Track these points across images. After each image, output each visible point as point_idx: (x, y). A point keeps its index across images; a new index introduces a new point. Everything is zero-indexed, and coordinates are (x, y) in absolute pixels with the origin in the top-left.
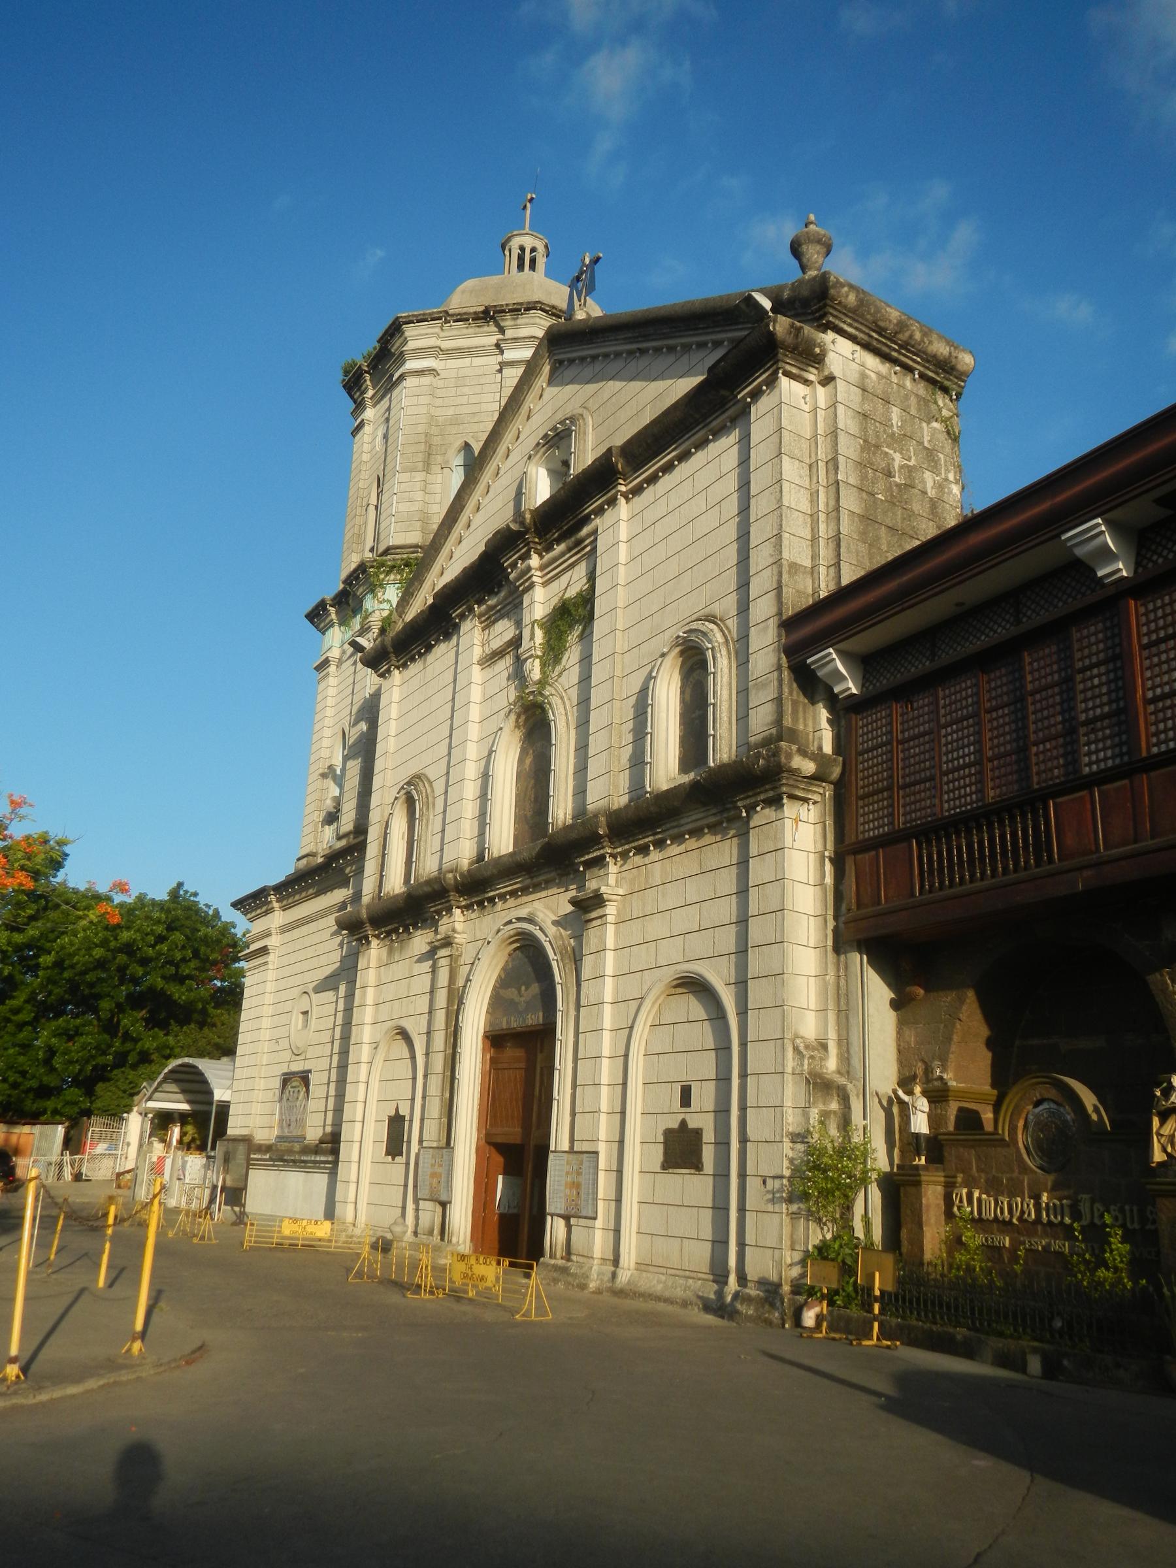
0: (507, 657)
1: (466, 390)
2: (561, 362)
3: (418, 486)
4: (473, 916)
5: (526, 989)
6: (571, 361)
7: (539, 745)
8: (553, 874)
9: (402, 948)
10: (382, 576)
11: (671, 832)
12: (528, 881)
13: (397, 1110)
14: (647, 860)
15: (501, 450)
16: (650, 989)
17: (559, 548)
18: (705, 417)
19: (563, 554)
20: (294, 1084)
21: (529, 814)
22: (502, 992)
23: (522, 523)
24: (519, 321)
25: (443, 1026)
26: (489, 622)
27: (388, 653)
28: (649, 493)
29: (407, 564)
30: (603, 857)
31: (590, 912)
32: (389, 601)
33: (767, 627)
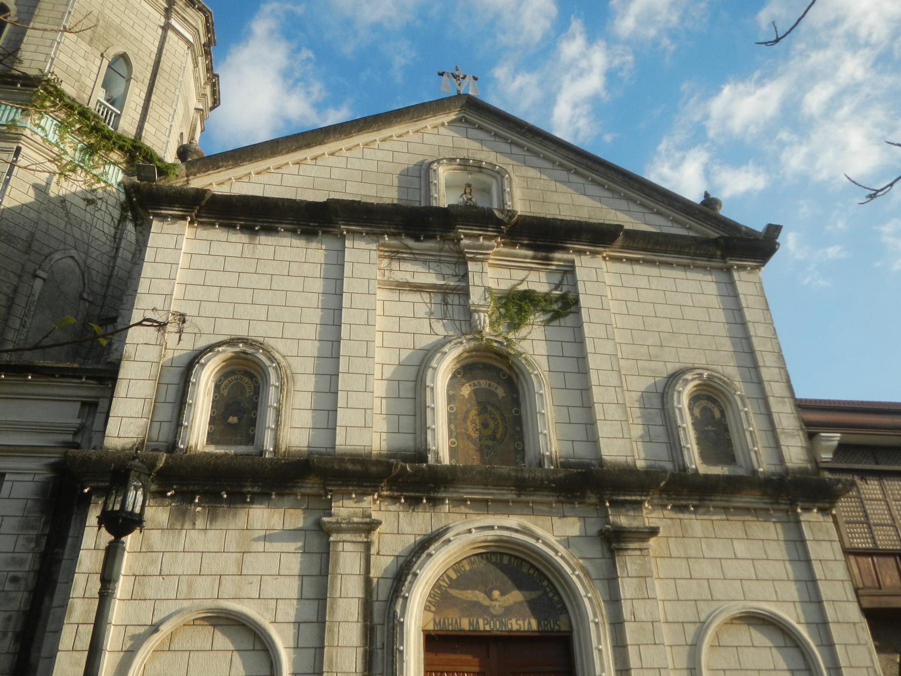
0: (426, 297)
1: (133, 16)
2: (467, 121)
3: (82, 54)
4: (392, 508)
5: (503, 594)
6: (480, 128)
7: (482, 382)
8: (551, 499)
9: (213, 517)
10: (48, 104)
11: (719, 503)
12: (514, 497)
14: (681, 516)
15: (386, 133)
16: (711, 617)
17: (518, 251)
18: (695, 255)
19: (526, 257)
21: (475, 436)
22: (454, 592)
23: (511, 218)
24: (188, 10)
26: (394, 255)
27: (199, 204)
28: (626, 268)
29: (80, 114)
30: (640, 503)
31: (624, 542)
32: (43, 129)
33: (784, 403)
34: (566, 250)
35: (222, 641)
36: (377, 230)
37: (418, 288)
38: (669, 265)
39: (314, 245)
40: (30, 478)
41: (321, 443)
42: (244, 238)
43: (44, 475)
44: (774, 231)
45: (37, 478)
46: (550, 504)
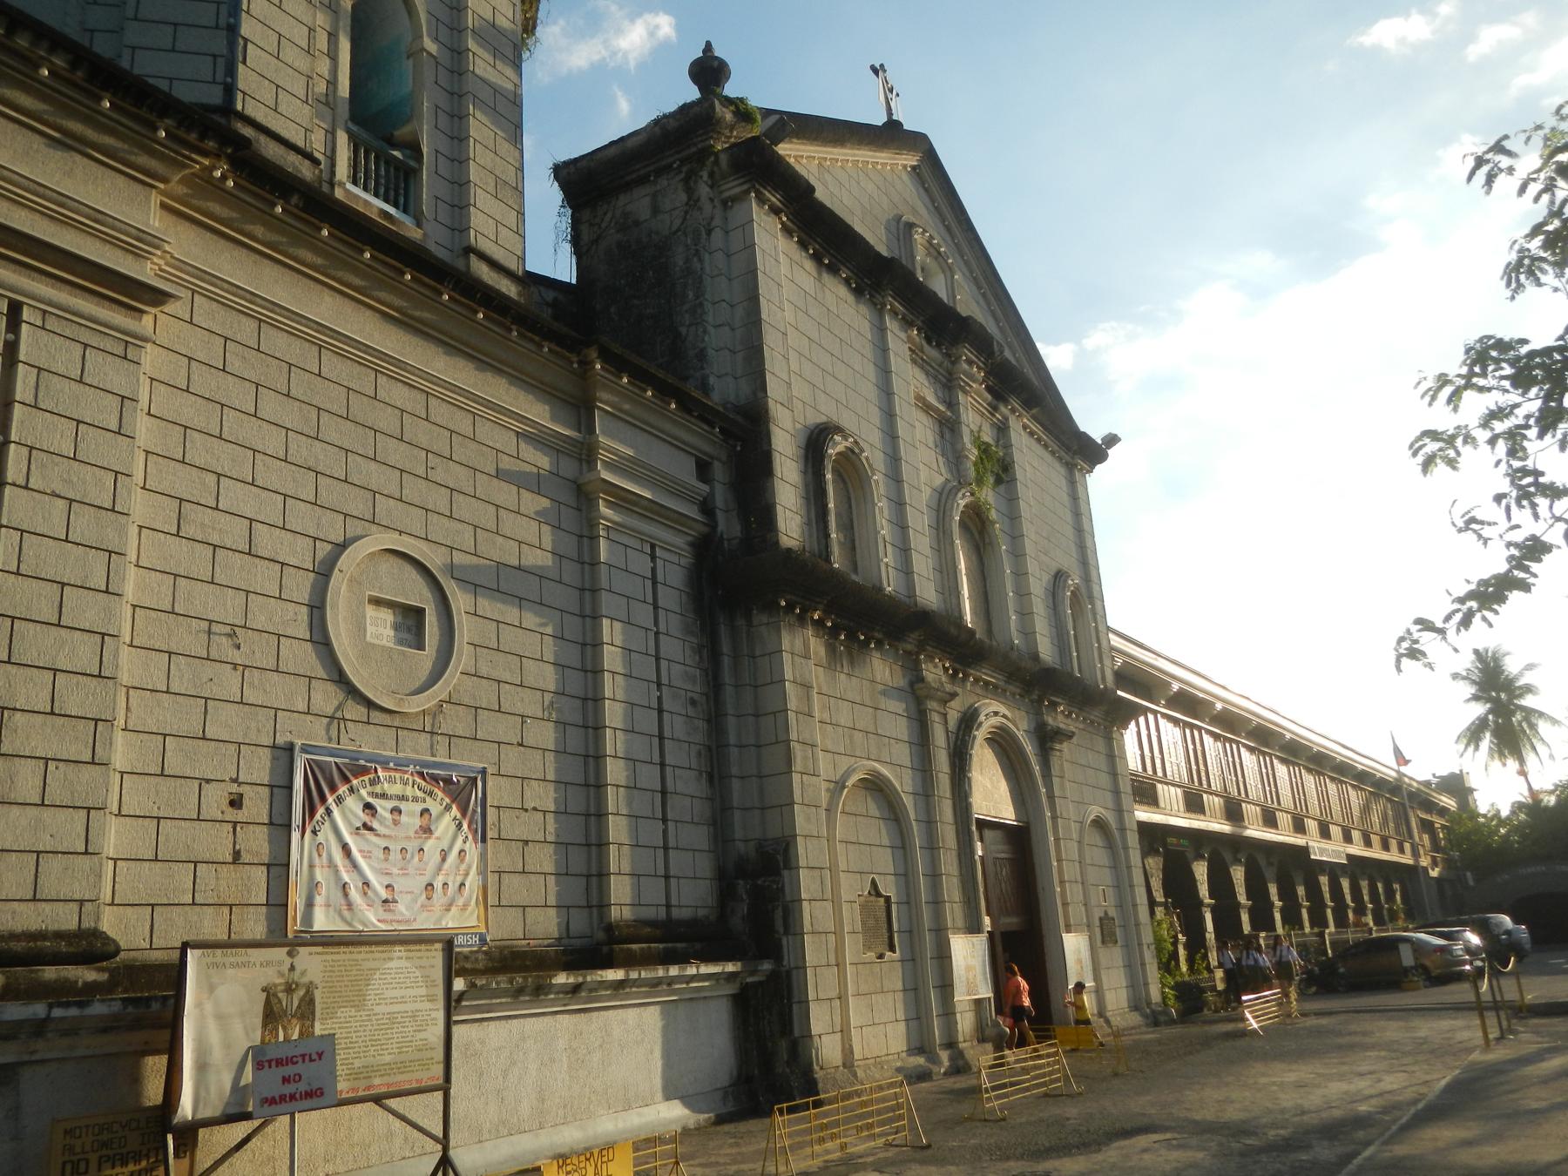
13: (874, 882)
20: (386, 787)
25: (948, 794)
34: (1006, 402)
35: (874, 810)
36: (910, 317)
37: (926, 408)
38: (1046, 446)
39: (864, 309)
40: (675, 559)
41: (903, 591)
42: (809, 265)
43: (687, 560)
44: (1112, 440)
45: (683, 561)
46: (1013, 695)
